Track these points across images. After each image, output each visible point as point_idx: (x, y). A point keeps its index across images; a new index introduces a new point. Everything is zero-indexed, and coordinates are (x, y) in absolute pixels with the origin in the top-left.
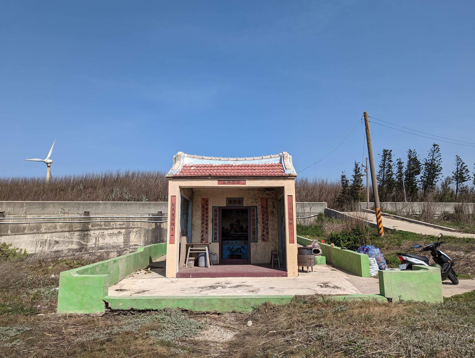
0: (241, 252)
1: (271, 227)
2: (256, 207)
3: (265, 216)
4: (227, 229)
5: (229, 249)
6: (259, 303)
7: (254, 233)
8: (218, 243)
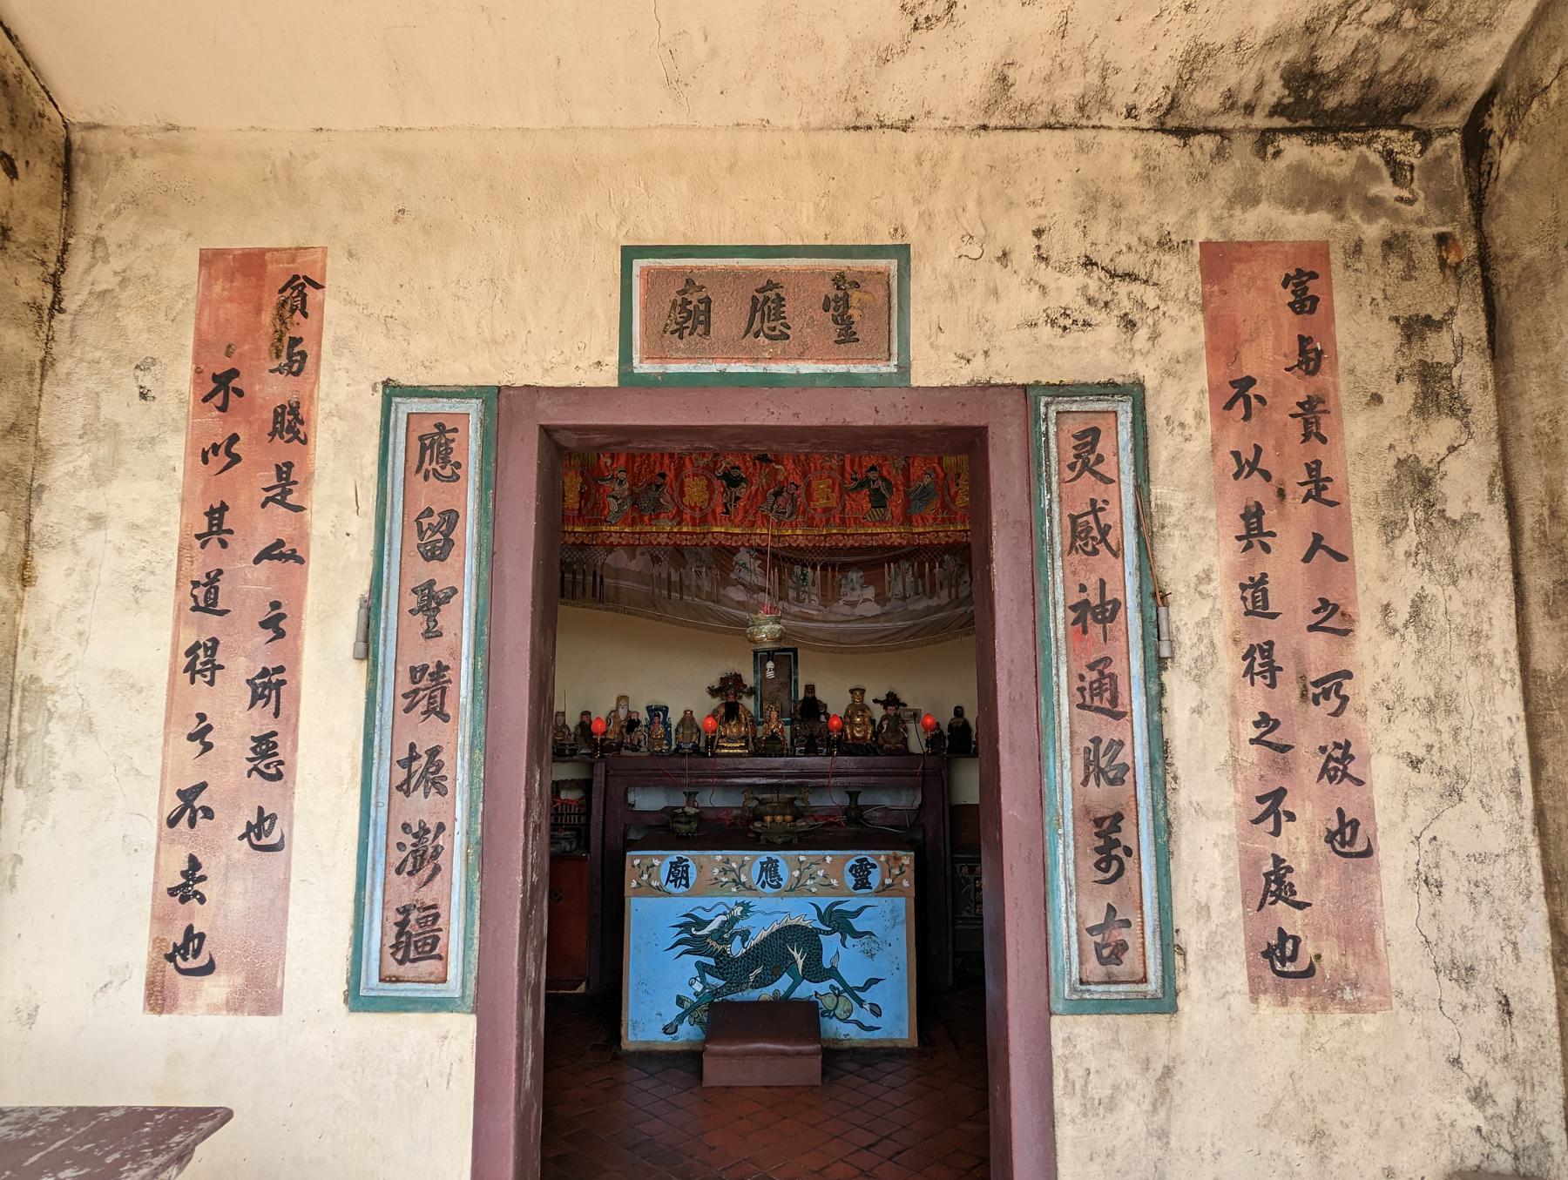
0: (815, 971)
1: (1409, 732)
2: (1135, 392)
3: (1289, 540)
4: (688, 720)
5: (692, 936)
7: (1108, 845)
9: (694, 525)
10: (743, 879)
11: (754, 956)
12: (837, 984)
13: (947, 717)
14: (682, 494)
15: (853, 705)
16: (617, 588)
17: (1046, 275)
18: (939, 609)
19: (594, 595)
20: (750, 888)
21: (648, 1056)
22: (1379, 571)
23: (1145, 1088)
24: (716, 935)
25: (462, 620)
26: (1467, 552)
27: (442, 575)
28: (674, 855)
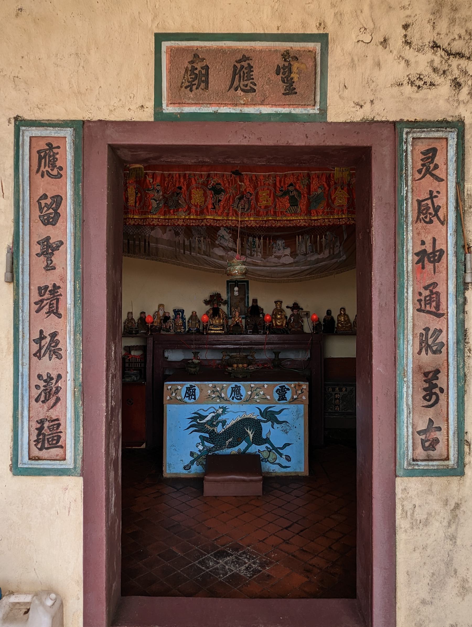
0: (259, 440)
4: (194, 316)
8: (75, 485)
9: (197, 215)
10: (223, 395)
11: (229, 433)
12: (269, 446)
13: (323, 315)
14: (190, 198)
15: (276, 309)
16: (157, 248)
17: (409, 53)
18: (323, 260)
19: (145, 252)
20: (226, 400)
21: (177, 481)
23: (445, 514)
24: (210, 423)
25: (67, 259)
27: (53, 233)
28: (188, 384)
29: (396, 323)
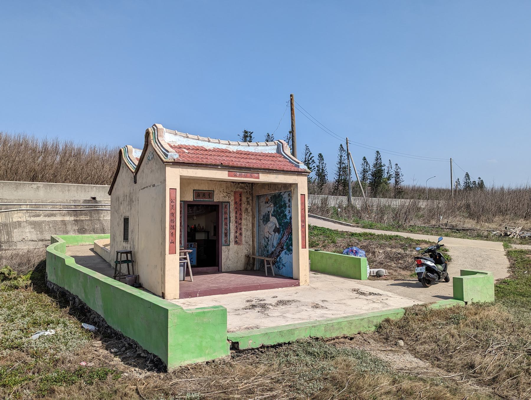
1: (245, 227)
2: (229, 202)
3: (238, 214)
6: (380, 321)
22: (244, 216)
26: (249, 215)
29: (222, 227)
